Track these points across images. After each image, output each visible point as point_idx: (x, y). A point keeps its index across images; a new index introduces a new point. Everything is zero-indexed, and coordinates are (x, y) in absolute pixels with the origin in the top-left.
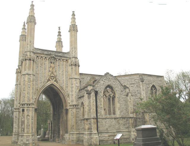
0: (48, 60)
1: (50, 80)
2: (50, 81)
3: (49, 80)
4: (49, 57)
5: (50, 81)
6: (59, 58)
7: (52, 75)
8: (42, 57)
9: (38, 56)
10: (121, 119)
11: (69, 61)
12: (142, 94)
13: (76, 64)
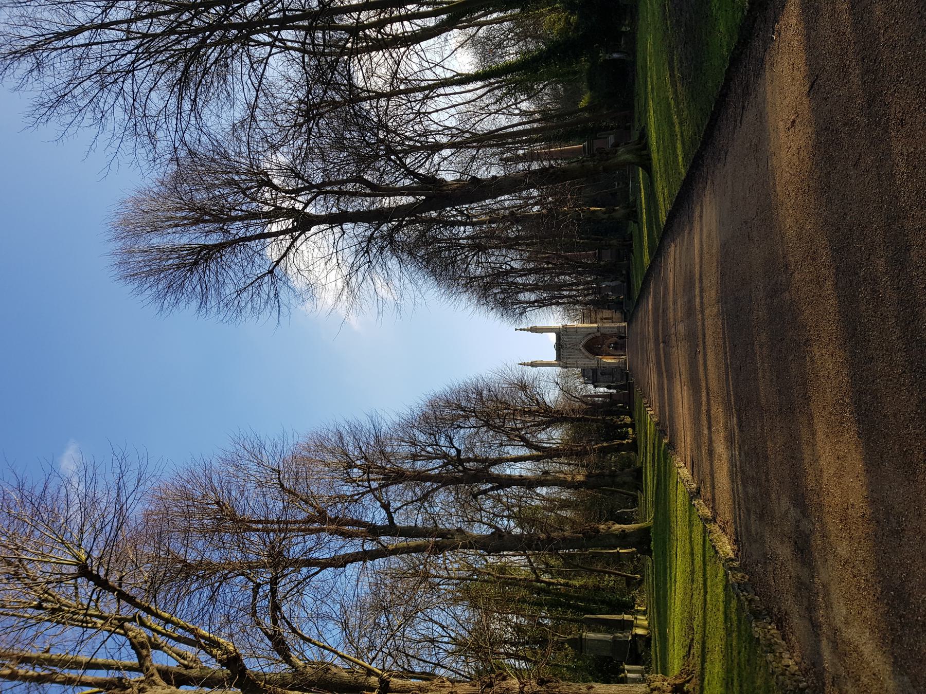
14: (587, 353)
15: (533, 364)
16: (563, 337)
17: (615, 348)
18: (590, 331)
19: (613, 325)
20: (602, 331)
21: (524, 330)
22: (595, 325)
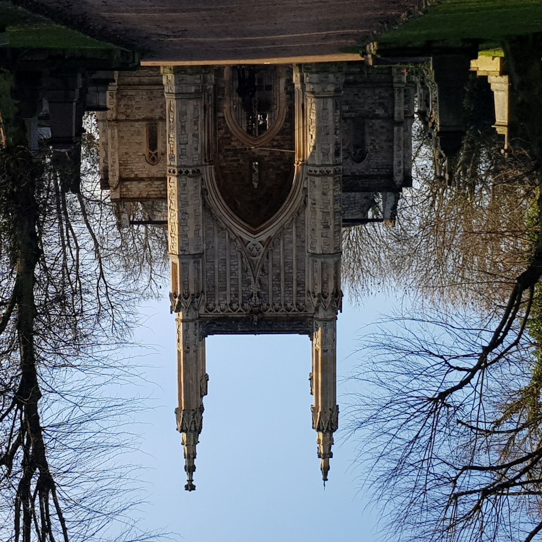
0: (268, 305)
2: (260, 242)
4: (267, 314)
5: (260, 242)
6: (236, 315)
9: (300, 310)
11: (202, 310)
13: (186, 299)
14: (283, 217)
15: (327, 421)
16: (221, 305)
17: (265, 107)
18: (195, 204)
19: (172, 117)
20: (195, 157)
21: (191, 456)
22: (172, 186)
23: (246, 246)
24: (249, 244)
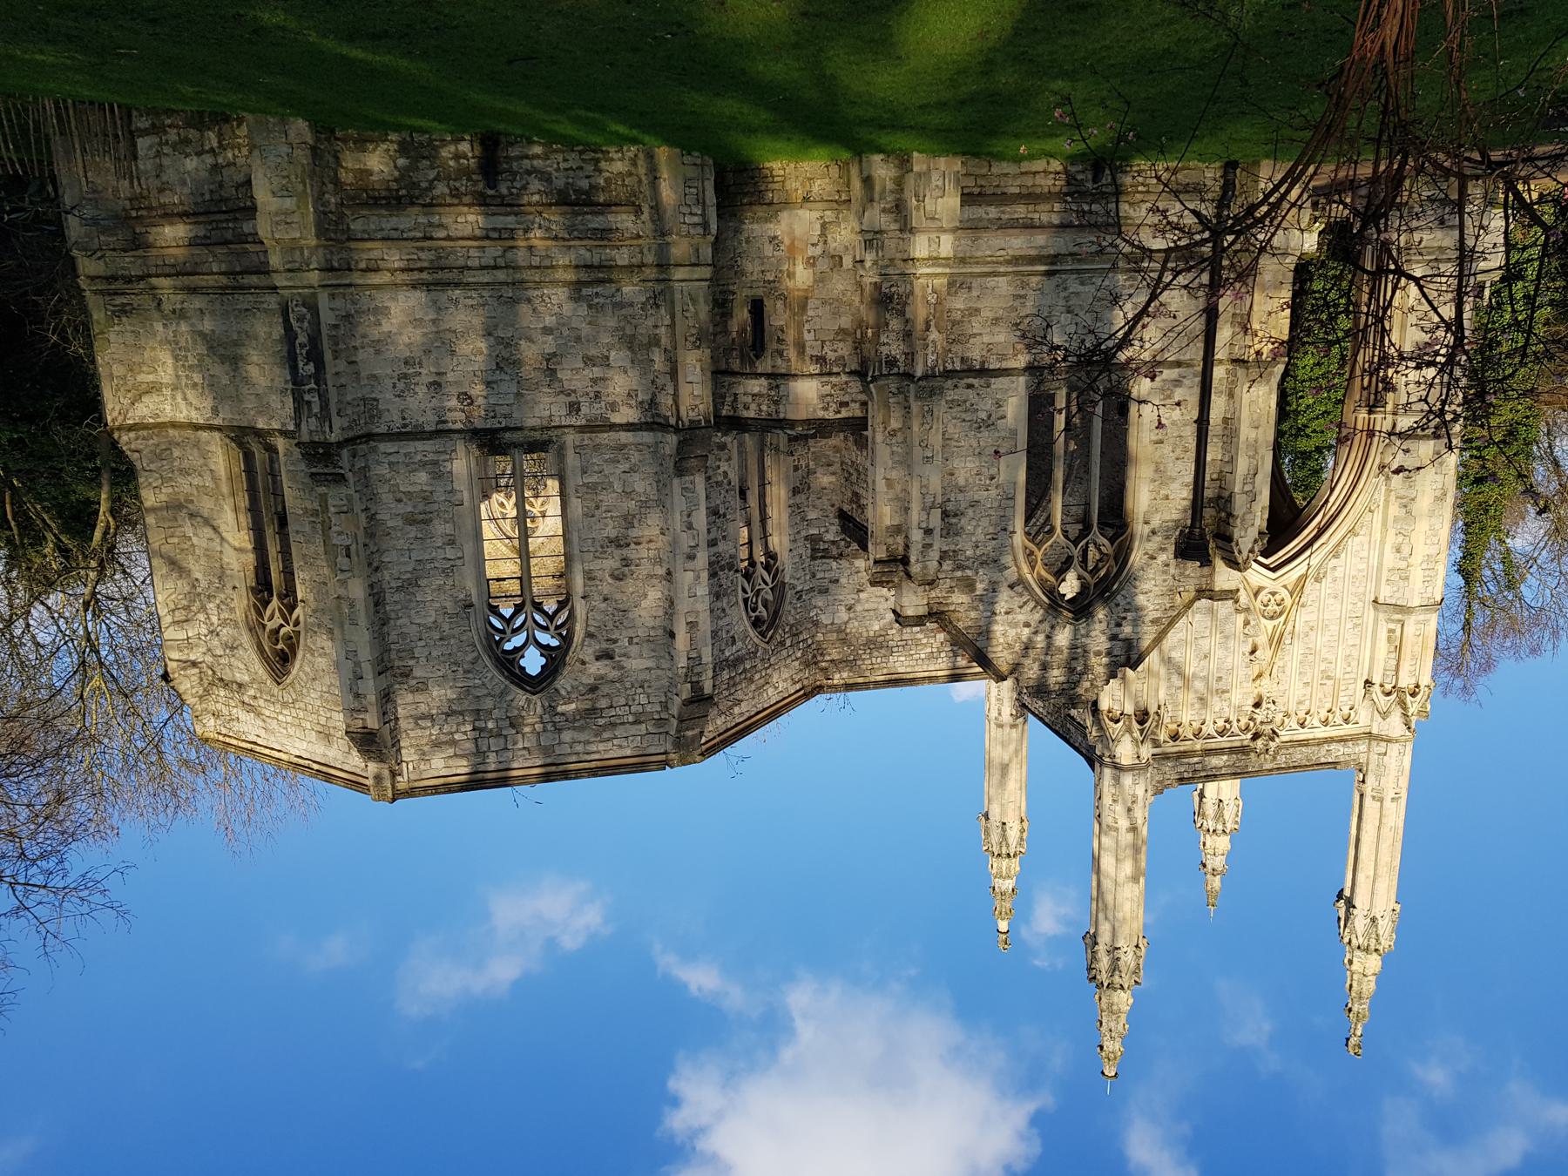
1: (1284, 594)
3: (1298, 588)
4: (1285, 736)
7: (1270, 624)
8: (1325, 723)
9: (1347, 721)
10: (994, 365)
12: (702, 590)
23: (1256, 595)
24: (1263, 596)
